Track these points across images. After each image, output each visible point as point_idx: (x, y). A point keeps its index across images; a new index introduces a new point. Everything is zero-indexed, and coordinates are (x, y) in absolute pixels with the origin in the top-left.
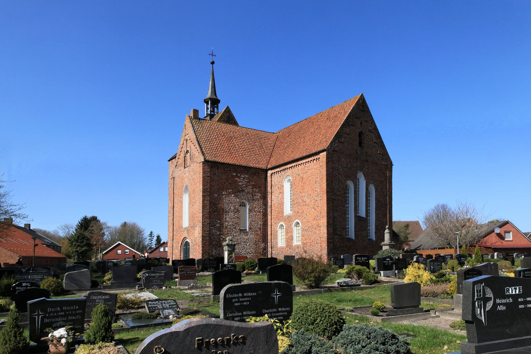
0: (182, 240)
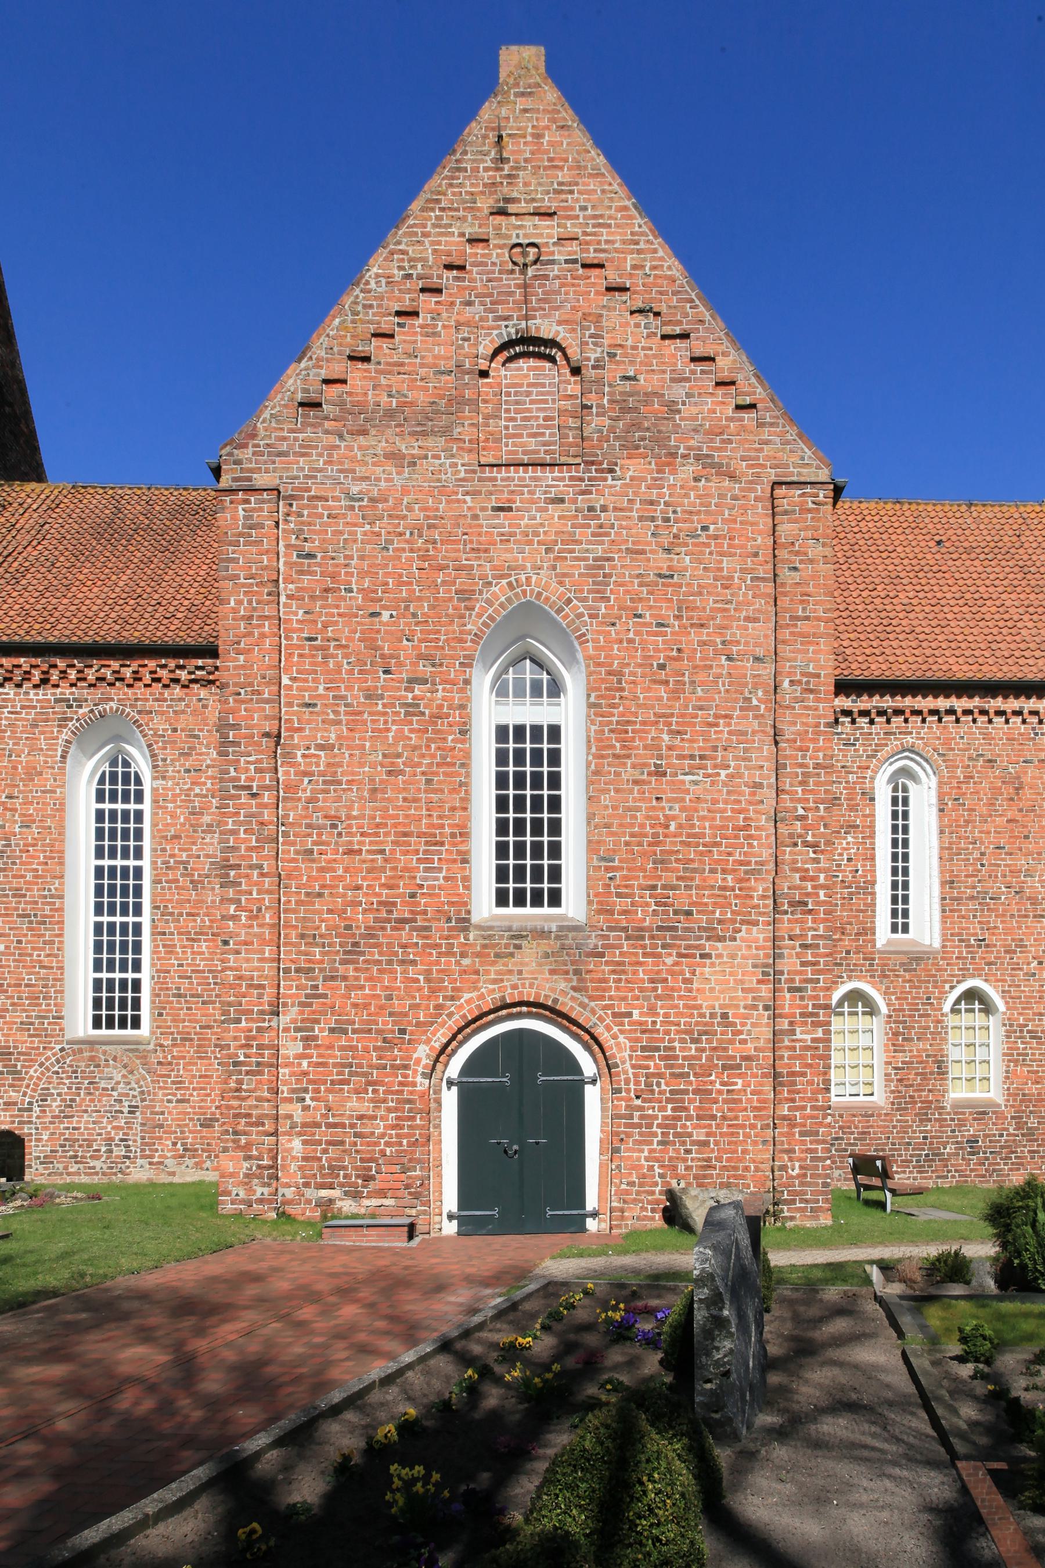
0: (454, 1023)
